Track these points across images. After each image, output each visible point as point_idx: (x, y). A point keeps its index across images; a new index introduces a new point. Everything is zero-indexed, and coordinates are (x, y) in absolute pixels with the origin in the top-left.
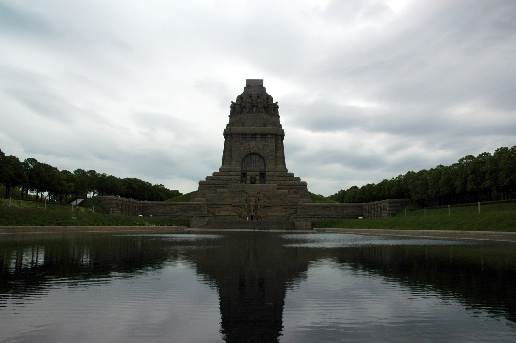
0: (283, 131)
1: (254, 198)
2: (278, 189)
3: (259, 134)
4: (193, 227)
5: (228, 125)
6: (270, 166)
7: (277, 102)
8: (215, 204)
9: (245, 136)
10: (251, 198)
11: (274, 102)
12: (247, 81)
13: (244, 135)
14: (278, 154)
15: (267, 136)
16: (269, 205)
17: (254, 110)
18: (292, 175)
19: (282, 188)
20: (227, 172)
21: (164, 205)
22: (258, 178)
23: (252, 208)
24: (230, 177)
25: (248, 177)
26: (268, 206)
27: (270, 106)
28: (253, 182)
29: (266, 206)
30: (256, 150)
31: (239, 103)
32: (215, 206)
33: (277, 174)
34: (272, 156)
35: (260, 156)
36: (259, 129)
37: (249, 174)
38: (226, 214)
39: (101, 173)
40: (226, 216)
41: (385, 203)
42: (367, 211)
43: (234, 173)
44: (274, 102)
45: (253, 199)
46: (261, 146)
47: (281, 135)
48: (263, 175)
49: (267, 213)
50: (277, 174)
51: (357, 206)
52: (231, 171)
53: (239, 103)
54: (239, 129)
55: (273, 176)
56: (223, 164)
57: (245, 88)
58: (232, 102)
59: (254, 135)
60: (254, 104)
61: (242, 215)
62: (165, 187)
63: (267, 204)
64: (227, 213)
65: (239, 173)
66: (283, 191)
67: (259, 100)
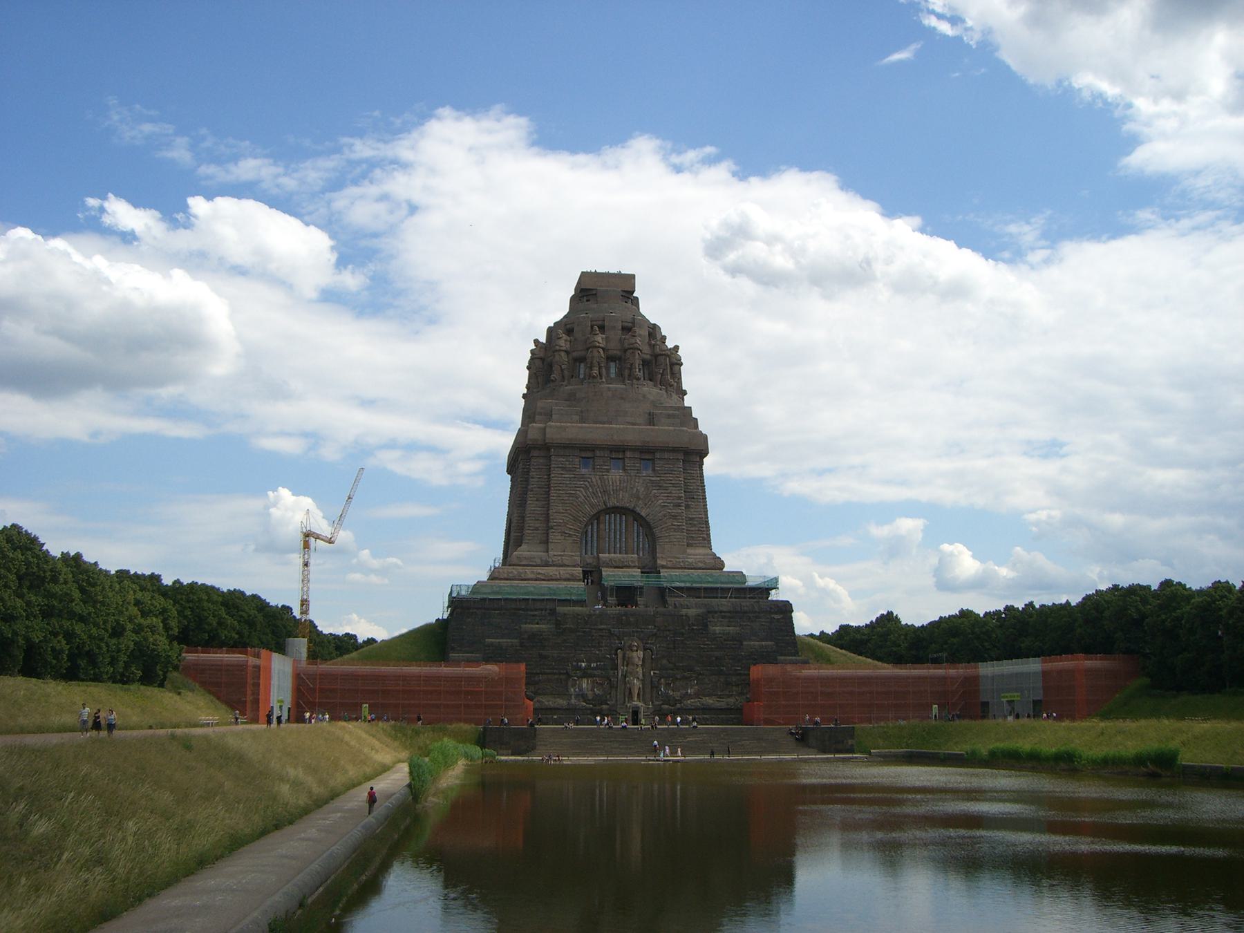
0: (705, 438)
7: (677, 348)
9: (589, 454)
11: (670, 344)
13: (587, 452)
15: (658, 455)
27: (661, 359)
30: (624, 499)
34: (674, 517)
35: (637, 517)
37: (606, 572)
38: (551, 704)
43: (563, 571)
44: (670, 344)
47: (696, 451)
58: (536, 341)
59: (618, 452)
60: (610, 352)
65: (578, 571)
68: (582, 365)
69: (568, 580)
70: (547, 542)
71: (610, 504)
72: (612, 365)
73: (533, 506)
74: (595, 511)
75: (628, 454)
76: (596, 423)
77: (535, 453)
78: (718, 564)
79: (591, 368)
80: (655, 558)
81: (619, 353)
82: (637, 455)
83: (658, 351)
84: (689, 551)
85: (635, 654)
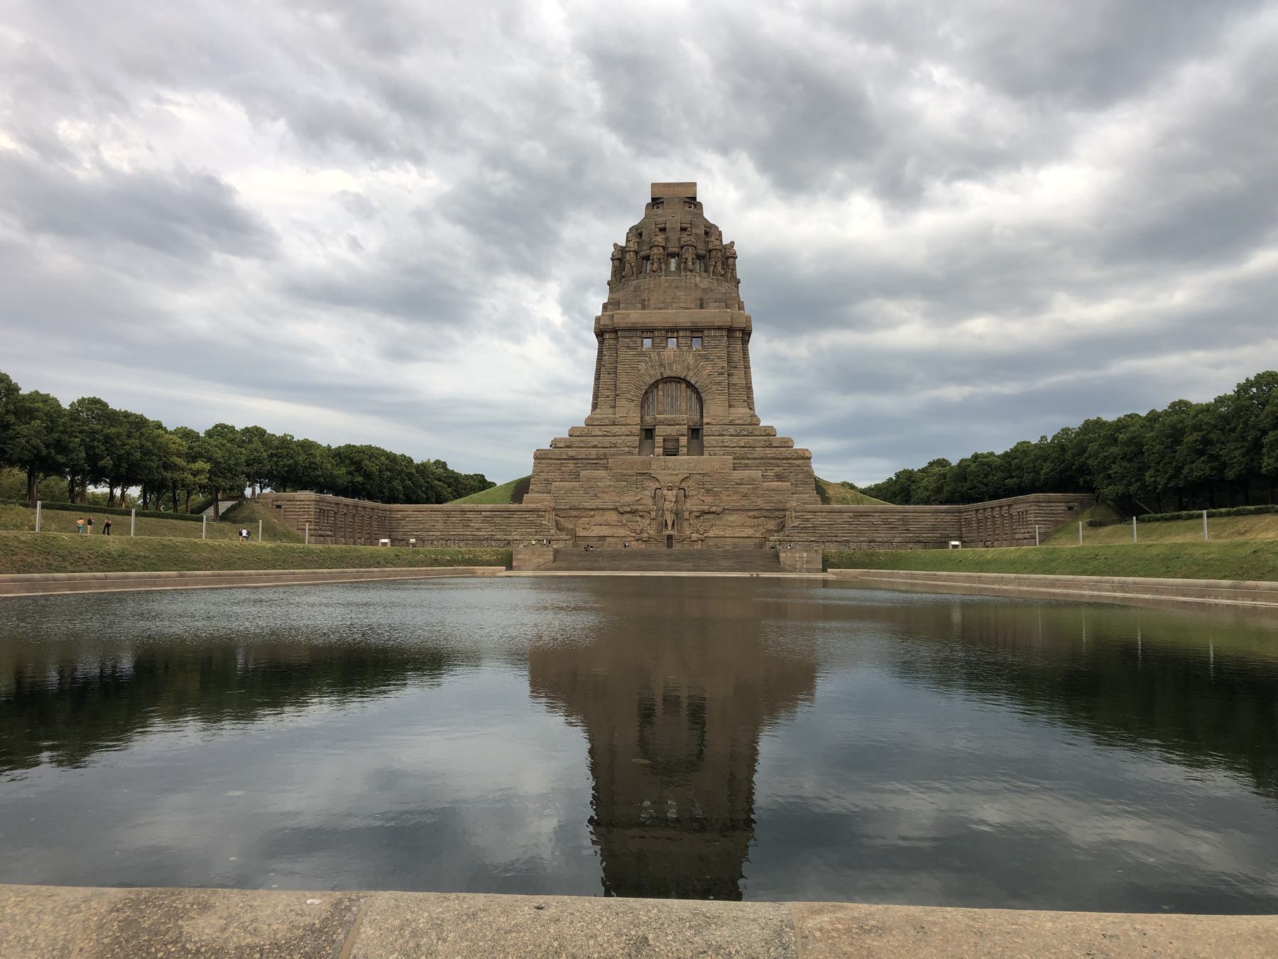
1: (675, 492)
3: (685, 329)
4: (519, 569)
5: (605, 307)
6: (715, 409)
7: (733, 243)
9: (649, 335)
10: (665, 492)
11: (726, 241)
12: (653, 185)
13: (647, 331)
14: (735, 380)
16: (714, 509)
17: (673, 263)
18: (769, 432)
20: (605, 428)
21: (448, 514)
22: (684, 441)
23: (669, 518)
24: (613, 440)
26: (709, 513)
27: (714, 253)
28: (671, 451)
29: (704, 513)
30: (677, 370)
31: (633, 246)
32: (574, 513)
33: (732, 430)
34: (719, 383)
35: (689, 385)
36: (684, 316)
37: (660, 431)
39: (279, 434)
40: (602, 538)
41: (1027, 504)
44: (726, 241)
45: (671, 495)
46: (690, 359)
48: (695, 432)
50: (732, 430)
51: (946, 512)
52: (614, 424)
53: (633, 246)
54: (635, 316)
56: (595, 406)
58: (615, 245)
59: (673, 330)
61: (645, 535)
64: (605, 531)
66: (747, 473)
67: (685, 238)
72: (673, 260)
73: (604, 378)
78: (754, 421)
80: (702, 416)
81: (676, 250)
82: (688, 334)
83: (711, 246)
84: (732, 410)
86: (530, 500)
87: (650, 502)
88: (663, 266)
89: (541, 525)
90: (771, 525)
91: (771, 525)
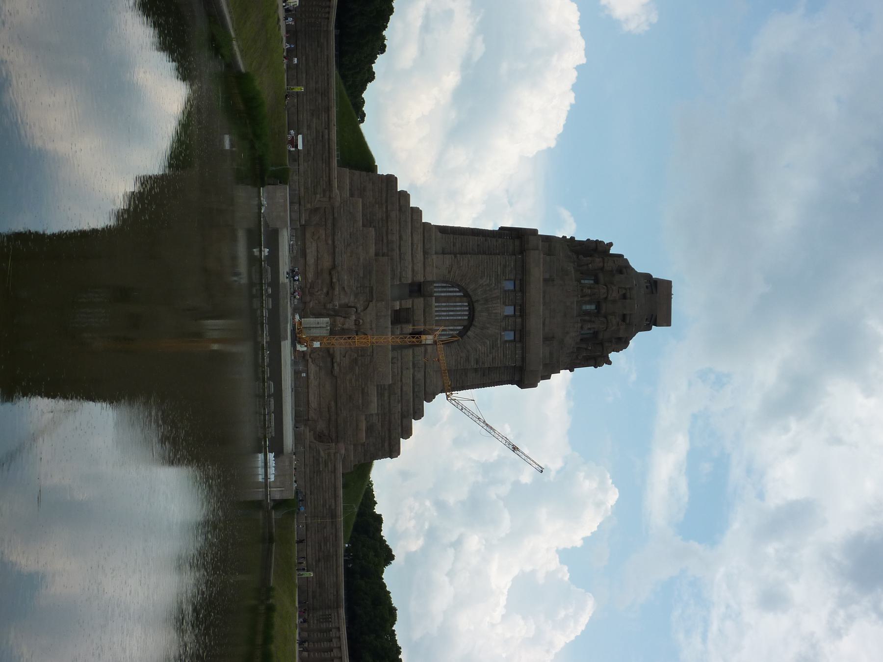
0: (534, 385)
2: (381, 391)
7: (609, 363)
8: (334, 225)
9: (517, 288)
10: (354, 317)
11: (612, 356)
12: (669, 283)
15: (518, 345)
17: (591, 307)
19: (380, 395)
20: (420, 246)
24: (408, 257)
25: (408, 304)
26: (333, 363)
30: (481, 317)
33: (420, 376)
34: (468, 359)
35: (466, 329)
36: (535, 324)
37: (419, 302)
42: (324, 626)
43: (419, 266)
44: (612, 356)
49: (313, 361)
52: (425, 253)
54: (537, 273)
55: (413, 364)
56: (444, 230)
57: (648, 276)
58: (611, 244)
62: (380, 57)
63: (338, 358)
65: (420, 278)
68: (592, 282)
69: (413, 270)
70: (443, 253)
71: (476, 305)
72: (593, 307)
74: (471, 293)
75: (519, 320)
76: (544, 292)
77: (517, 242)
78: (430, 398)
79: (590, 288)
81: (603, 311)
85: (353, 323)
86: (342, 179)
87: (344, 300)
88: (587, 299)
89: (315, 193)
90: (321, 426)
91: (321, 426)
